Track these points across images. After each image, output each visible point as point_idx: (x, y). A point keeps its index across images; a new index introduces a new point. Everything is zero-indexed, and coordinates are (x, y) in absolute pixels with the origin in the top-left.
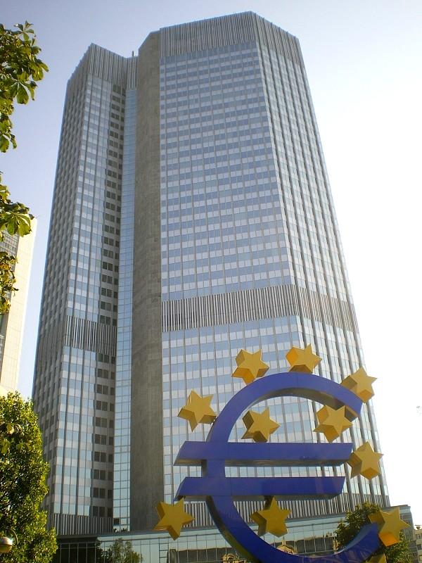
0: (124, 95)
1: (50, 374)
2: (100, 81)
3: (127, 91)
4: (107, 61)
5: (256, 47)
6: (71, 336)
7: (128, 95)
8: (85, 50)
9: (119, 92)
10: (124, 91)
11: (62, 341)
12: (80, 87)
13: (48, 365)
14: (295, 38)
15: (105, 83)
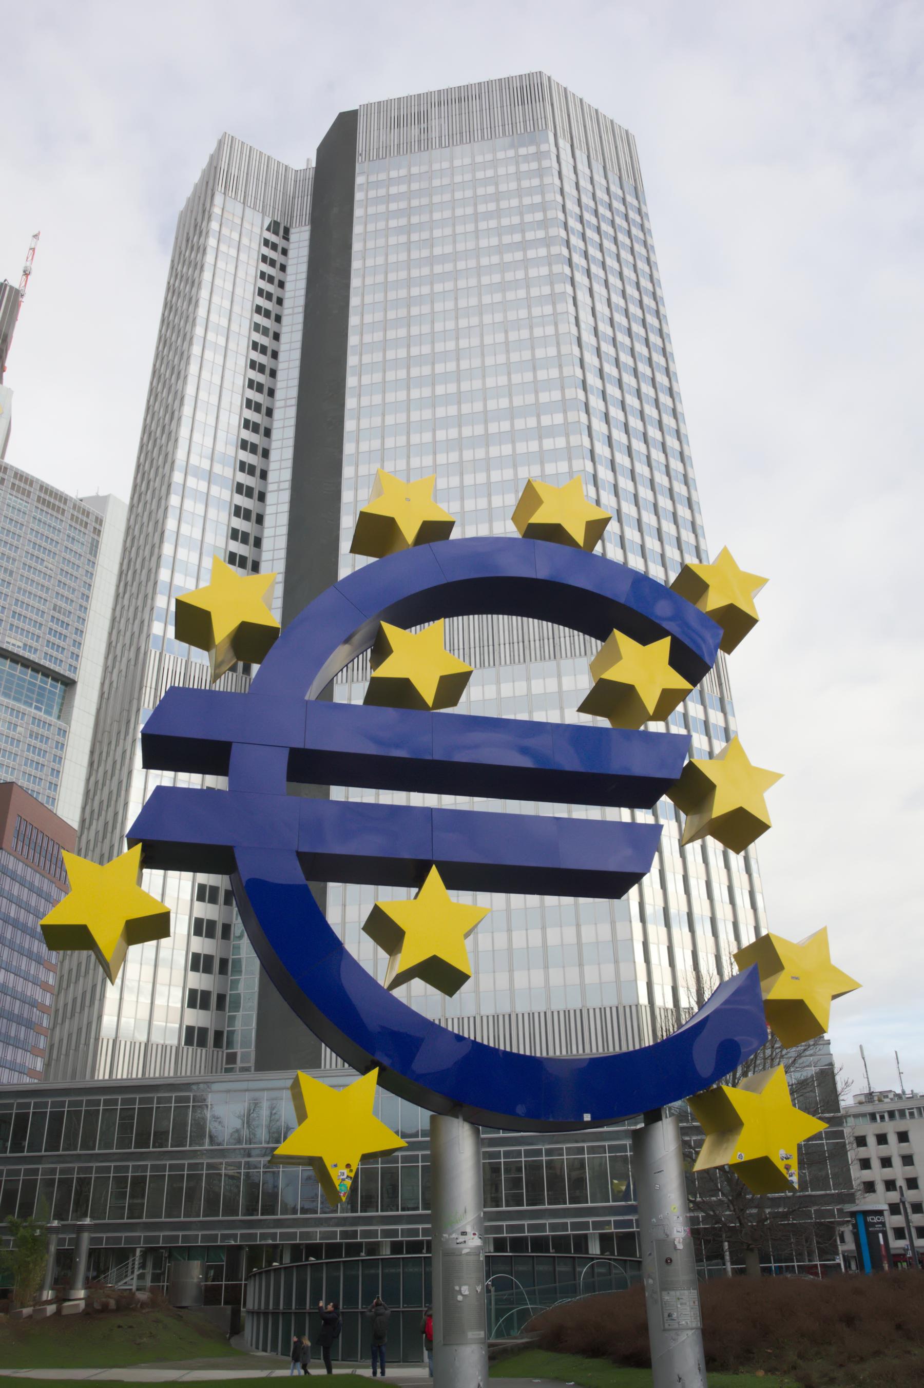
0: (286, 237)
1: (115, 762)
2: (239, 207)
3: (292, 231)
4: (254, 163)
5: (547, 141)
6: (156, 689)
7: (293, 237)
8: (212, 148)
9: (276, 233)
10: (287, 231)
11: (139, 699)
12: (199, 220)
13: (113, 747)
14: (628, 138)
15: (248, 210)
